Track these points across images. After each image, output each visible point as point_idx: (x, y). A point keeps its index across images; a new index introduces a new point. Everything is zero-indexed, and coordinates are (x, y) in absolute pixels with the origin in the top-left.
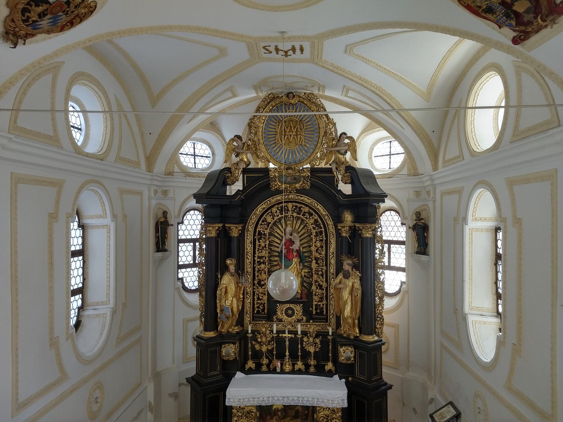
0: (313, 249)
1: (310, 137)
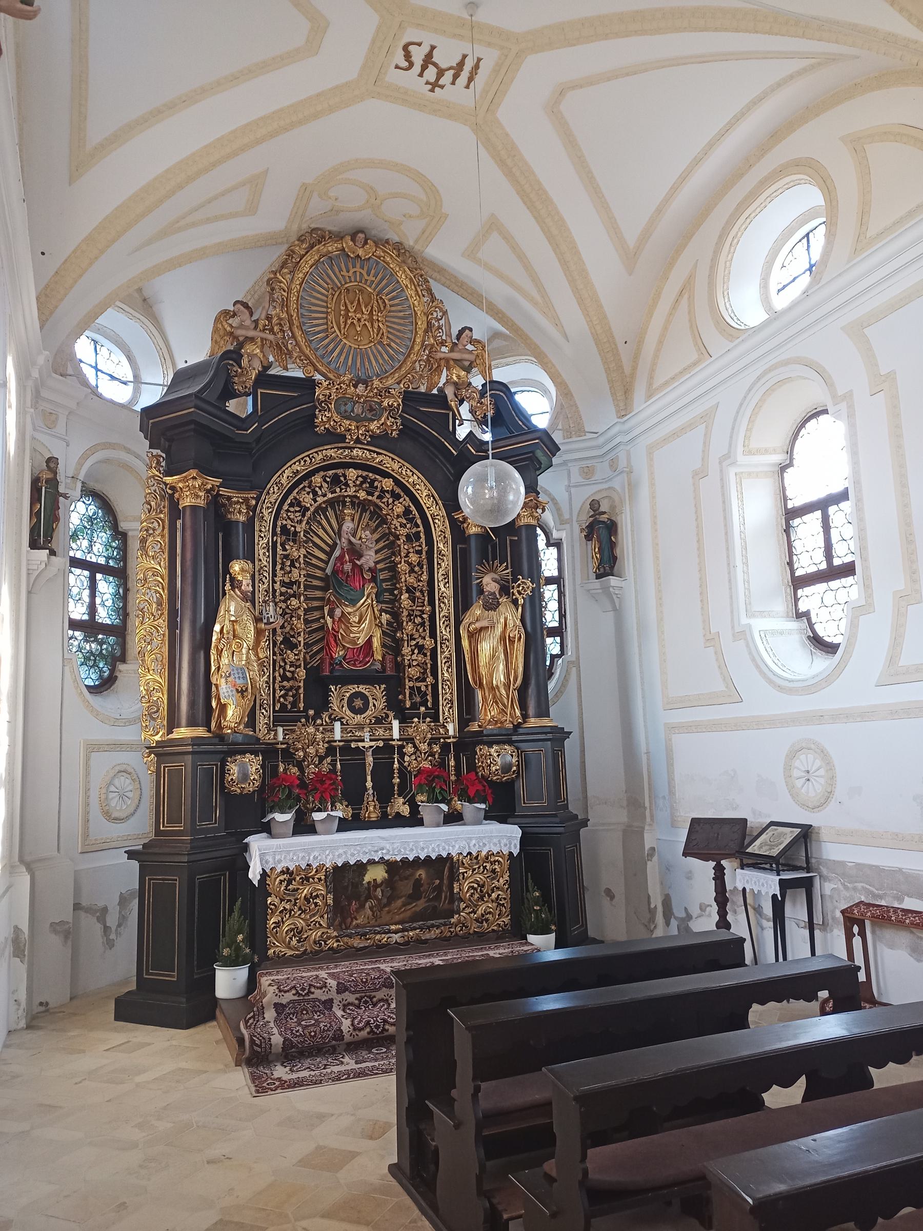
0: (403, 567)
1: (399, 331)
